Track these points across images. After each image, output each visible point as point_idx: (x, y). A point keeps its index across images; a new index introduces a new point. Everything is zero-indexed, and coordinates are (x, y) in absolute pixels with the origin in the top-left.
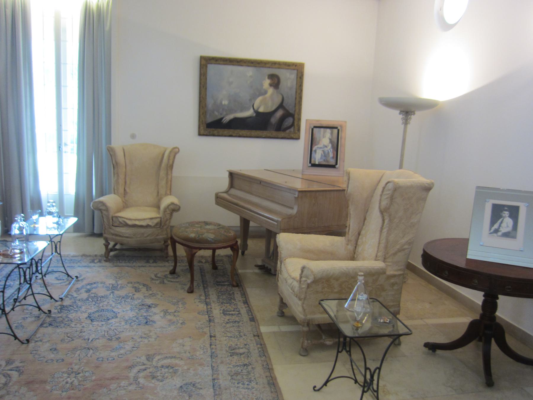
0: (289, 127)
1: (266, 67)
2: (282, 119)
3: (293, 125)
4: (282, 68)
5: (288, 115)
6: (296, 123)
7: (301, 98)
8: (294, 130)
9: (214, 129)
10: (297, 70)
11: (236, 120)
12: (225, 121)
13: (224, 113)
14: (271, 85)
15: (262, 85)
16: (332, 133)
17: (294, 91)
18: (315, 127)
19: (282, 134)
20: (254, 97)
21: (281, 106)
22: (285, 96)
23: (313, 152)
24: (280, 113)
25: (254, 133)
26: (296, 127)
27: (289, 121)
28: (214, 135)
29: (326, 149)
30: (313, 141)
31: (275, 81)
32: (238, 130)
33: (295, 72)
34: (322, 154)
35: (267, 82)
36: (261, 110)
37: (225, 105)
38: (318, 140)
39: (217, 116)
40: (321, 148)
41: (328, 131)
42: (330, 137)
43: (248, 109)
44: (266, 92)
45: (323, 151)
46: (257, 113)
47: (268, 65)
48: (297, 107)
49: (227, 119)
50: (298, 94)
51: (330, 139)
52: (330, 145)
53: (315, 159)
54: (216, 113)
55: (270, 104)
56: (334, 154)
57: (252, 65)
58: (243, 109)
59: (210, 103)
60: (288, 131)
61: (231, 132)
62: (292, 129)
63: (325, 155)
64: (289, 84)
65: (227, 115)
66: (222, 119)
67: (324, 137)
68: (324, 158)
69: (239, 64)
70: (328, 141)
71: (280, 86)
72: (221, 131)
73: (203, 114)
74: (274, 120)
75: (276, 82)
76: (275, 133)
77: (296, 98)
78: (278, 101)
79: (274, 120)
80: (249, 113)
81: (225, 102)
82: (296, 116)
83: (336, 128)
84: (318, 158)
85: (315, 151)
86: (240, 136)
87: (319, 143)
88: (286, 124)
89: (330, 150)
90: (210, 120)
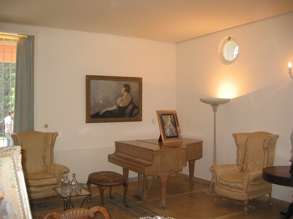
1: (122, 81)
3: (138, 112)
4: (131, 81)
6: (139, 113)
9: (95, 119)
10: (139, 82)
11: (107, 111)
14: (125, 91)
15: (121, 91)
17: (138, 93)
19: (133, 119)
20: (117, 98)
21: (131, 102)
22: (133, 97)
23: (165, 130)
24: (131, 107)
25: (117, 119)
27: (136, 111)
28: (95, 122)
29: (170, 127)
31: (128, 88)
32: (109, 118)
33: (138, 82)
35: (123, 89)
36: (121, 105)
37: (101, 104)
38: (165, 122)
39: (97, 110)
40: (168, 127)
43: (114, 105)
44: (123, 95)
45: (170, 128)
47: (123, 80)
52: (172, 125)
54: (96, 109)
56: (175, 130)
59: (92, 102)
60: (136, 117)
61: (105, 119)
62: (138, 116)
63: (171, 130)
64: (135, 90)
65: (102, 109)
66: (100, 112)
72: (99, 119)
74: (128, 111)
76: (129, 118)
77: (139, 98)
78: (129, 99)
79: (128, 111)
80: (114, 108)
81: (101, 102)
82: (139, 107)
85: (166, 129)
88: (135, 112)
90: (92, 113)
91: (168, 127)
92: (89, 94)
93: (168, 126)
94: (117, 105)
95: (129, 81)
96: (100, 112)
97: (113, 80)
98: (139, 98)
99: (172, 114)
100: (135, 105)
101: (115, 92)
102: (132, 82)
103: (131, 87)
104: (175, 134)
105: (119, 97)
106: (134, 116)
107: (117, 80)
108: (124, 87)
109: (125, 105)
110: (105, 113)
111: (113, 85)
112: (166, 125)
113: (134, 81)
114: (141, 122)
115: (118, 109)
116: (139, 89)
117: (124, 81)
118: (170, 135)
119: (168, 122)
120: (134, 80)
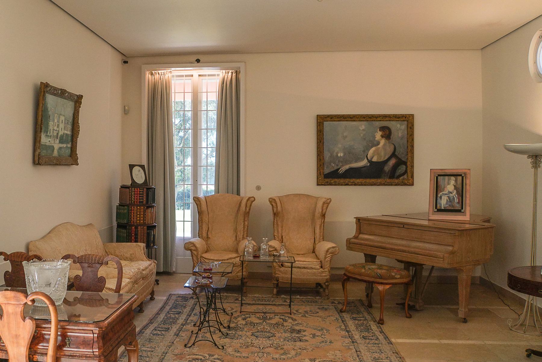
0: (403, 174)
1: (376, 121)
2: (395, 168)
3: (406, 172)
5: (401, 162)
6: (409, 171)
7: (413, 146)
8: (407, 176)
10: (407, 121)
11: (351, 169)
12: (342, 171)
13: (341, 164)
15: (374, 137)
16: (456, 181)
17: (406, 140)
18: (439, 175)
19: (396, 181)
20: (368, 148)
21: (393, 155)
22: (396, 146)
23: (438, 198)
24: (393, 162)
26: (410, 175)
27: (402, 168)
28: (331, 184)
29: (452, 195)
30: (437, 189)
31: (387, 133)
33: (406, 122)
34: (447, 200)
35: (378, 135)
36: (375, 159)
38: (443, 187)
39: (333, 167)
40: (446, 194)
41: (453, 178)
42: (455, 185)
43: (362, 160)
44: (378, 143)
46: (370, 162)
47: (379, 119)
48: (409, 155)
49: (343, 170)
50: (409, 143)
51: (454, 186)
52: (455, 192)
53: (441, 204)
55: (383, 154)
57: (364, 119)
58: (357, 160)
59: (327, 155)
61: (347, 181)
62: (405, 176)
63: (450, 200)
64: (400, 135)
65: (343, 166)
66: (339, 169)
67: (449, 184)
68: (449, 203)
69: (352, 120)
70: (453, 187)
71: (391, 137)
73: (321, 165)
74: (387, 168)
75: (387, 133)
76: (388, 180)
77: (408, 147)
79: (387, 168)
80: (364, 163)
81: (341, 154)
82: (408, 163)
83: (461, 175)
84: (443, 202)
85: (441, 197)
86: (355, 185)
87: (443, 190)
88: (399, 171)
89: (456, 196)
90: (327, 171)
91: (446, 194)
92: (322, 142)
93: (447, 192)
94: (367, 159)
95: (389, 121)
96: (339, 171)
97: (361, 121)
98: (408, 147)
99: (461, 175)
100: (400, 159)
101: (365, 139)
102: (394, 123)
103: (392, 132)
104: (458, 207)
105: (372, 147)
106: (398, 177)
107: (368, 121)
108: (380, 130)
109: (382, 159)
110: (347, 171)
111: (361, 129)
112: (444, 191)
113: (398, 121)
114: (413, 186)
115: (370, 165)
116: (408, 134)
117: (381, 121)
118: (446, 207)
119: (448, 186)
120: (397, 120)
